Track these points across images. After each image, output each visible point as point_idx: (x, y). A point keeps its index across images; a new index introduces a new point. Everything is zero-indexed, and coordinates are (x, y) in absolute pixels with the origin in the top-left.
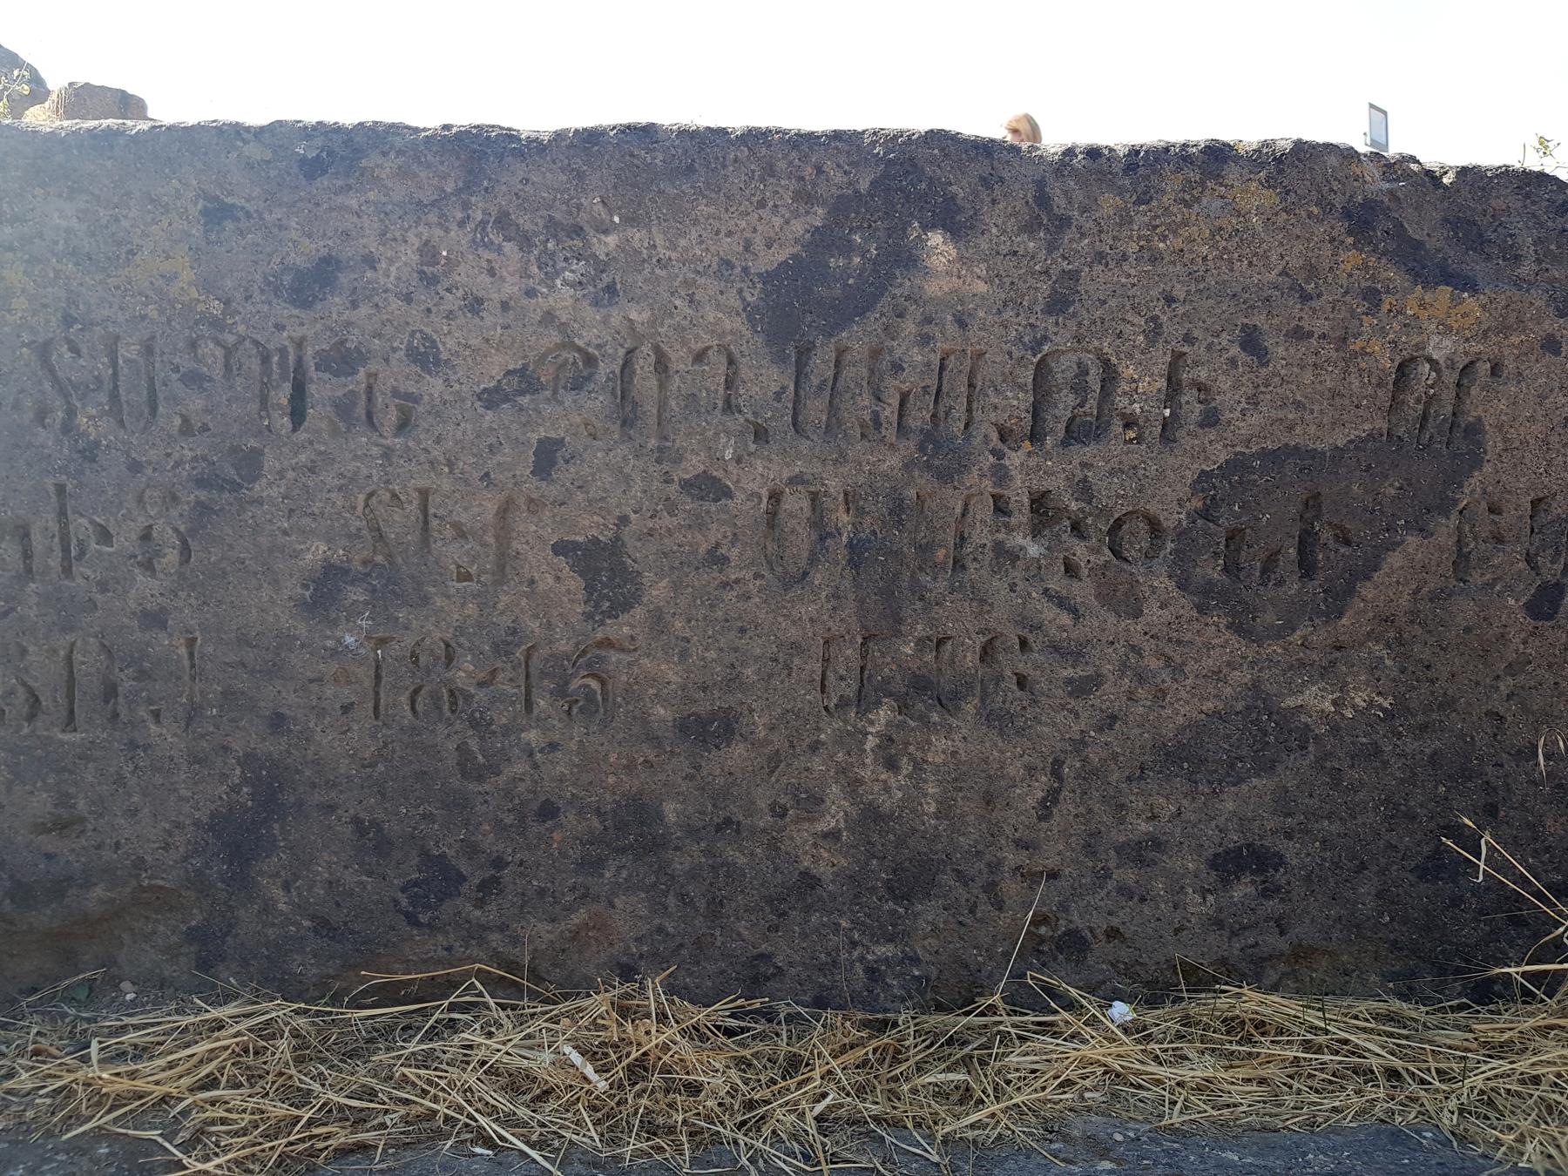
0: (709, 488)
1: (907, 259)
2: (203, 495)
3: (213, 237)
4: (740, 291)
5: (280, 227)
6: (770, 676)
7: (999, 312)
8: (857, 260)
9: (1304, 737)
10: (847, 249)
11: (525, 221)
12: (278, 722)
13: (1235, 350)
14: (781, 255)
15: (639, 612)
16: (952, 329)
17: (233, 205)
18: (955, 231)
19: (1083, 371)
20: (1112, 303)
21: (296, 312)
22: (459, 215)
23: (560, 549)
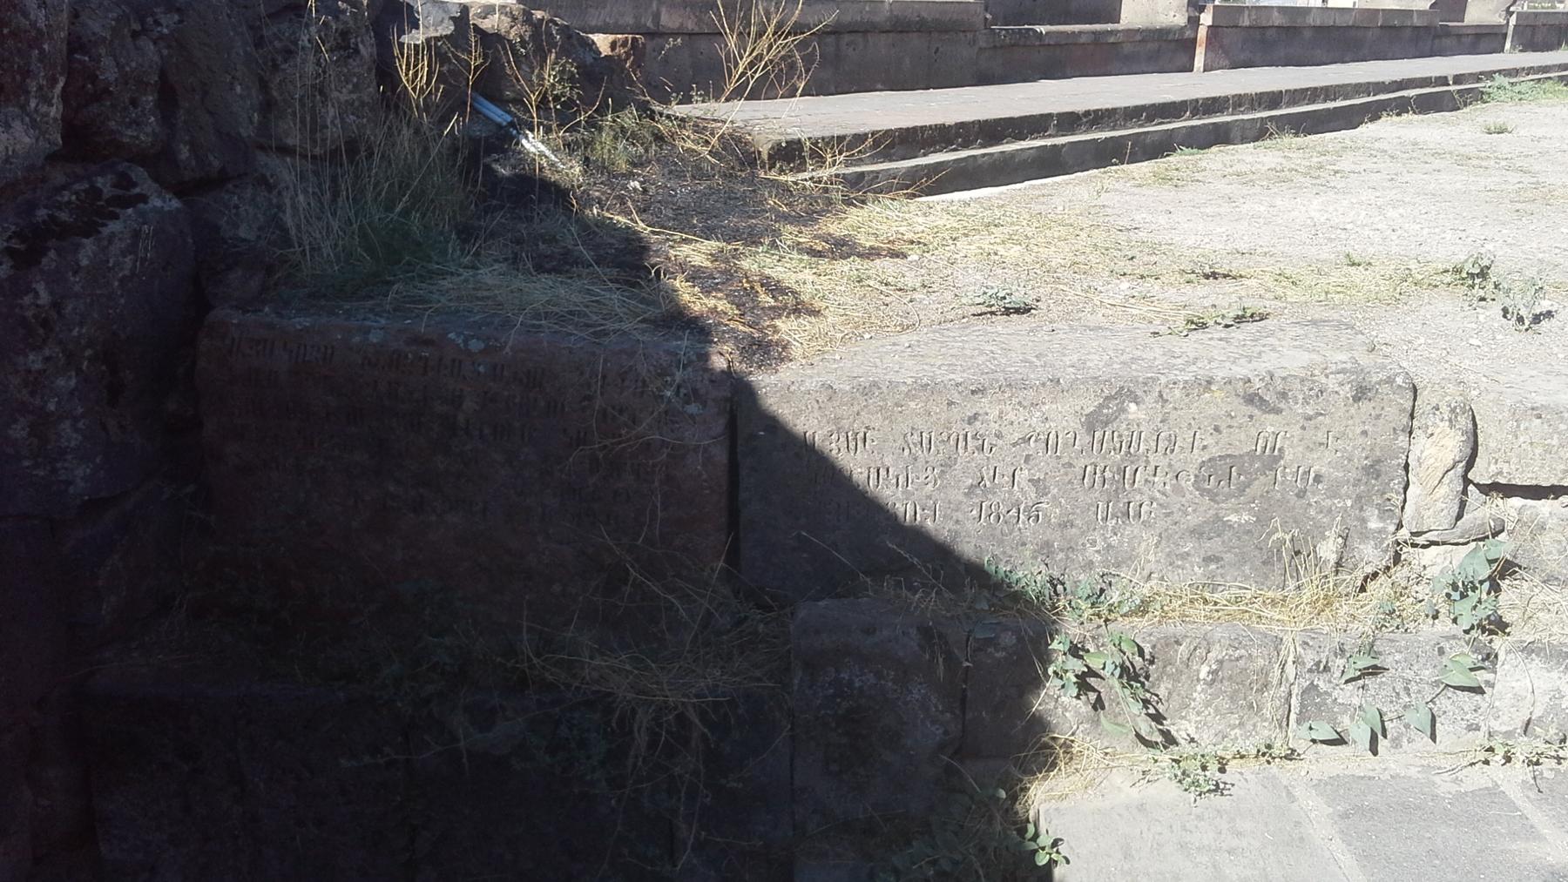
1: (1124, 410)
10: (1108, 408)
12: (957, 522)
14: (1092, 409)
18: (1137, 404)
19: (1170, 435)
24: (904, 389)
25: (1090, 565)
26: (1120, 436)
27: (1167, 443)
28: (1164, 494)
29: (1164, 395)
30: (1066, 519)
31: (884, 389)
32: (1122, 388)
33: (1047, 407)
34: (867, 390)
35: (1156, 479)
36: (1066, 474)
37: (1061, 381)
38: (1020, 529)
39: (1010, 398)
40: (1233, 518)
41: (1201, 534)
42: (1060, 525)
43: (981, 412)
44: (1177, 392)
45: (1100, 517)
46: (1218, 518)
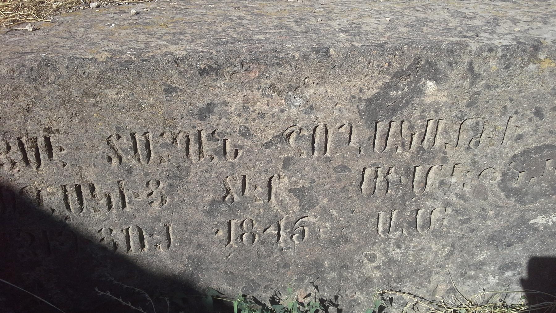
0: (344, 168)
1: (418, 91)
2: (170, 181)
3: (169, 98)
4: (358, 106)
5: (193, 94)
6: (360, 224)
7: (450, 107)
8: (400, 92)
9: (536, 230)
10: (397, 89)
11: (280, 87)
12: (199, 246)
13: (532, 115)
14: (374, 91)
15: (317, 207)
16: (432, 113)
17: (175, 87)
18: (437, 81)
20: (491, 102)
21: (200, 122)
22: (257, 86)
23: (290, 191)
24: (92, 69)
25: (367, 282)
26: (411, 127)
27: (471, 133)
28: (462, 197)
29: (476, 68)
30: (338, 234)
31: (63, 70)
32: (418, 59)
33: (312, 91)
34: (35, 74)
35: (454, 180)
36: (339, 180)
37: (331, 50)
38: (281, 250)
39: (258, 80)
40: (540, 220)
41: (500, 241)
42: (331, 241)
43: (217, 101)
44: (493, 64)
45: (380, 229)
46: (523, 221)
